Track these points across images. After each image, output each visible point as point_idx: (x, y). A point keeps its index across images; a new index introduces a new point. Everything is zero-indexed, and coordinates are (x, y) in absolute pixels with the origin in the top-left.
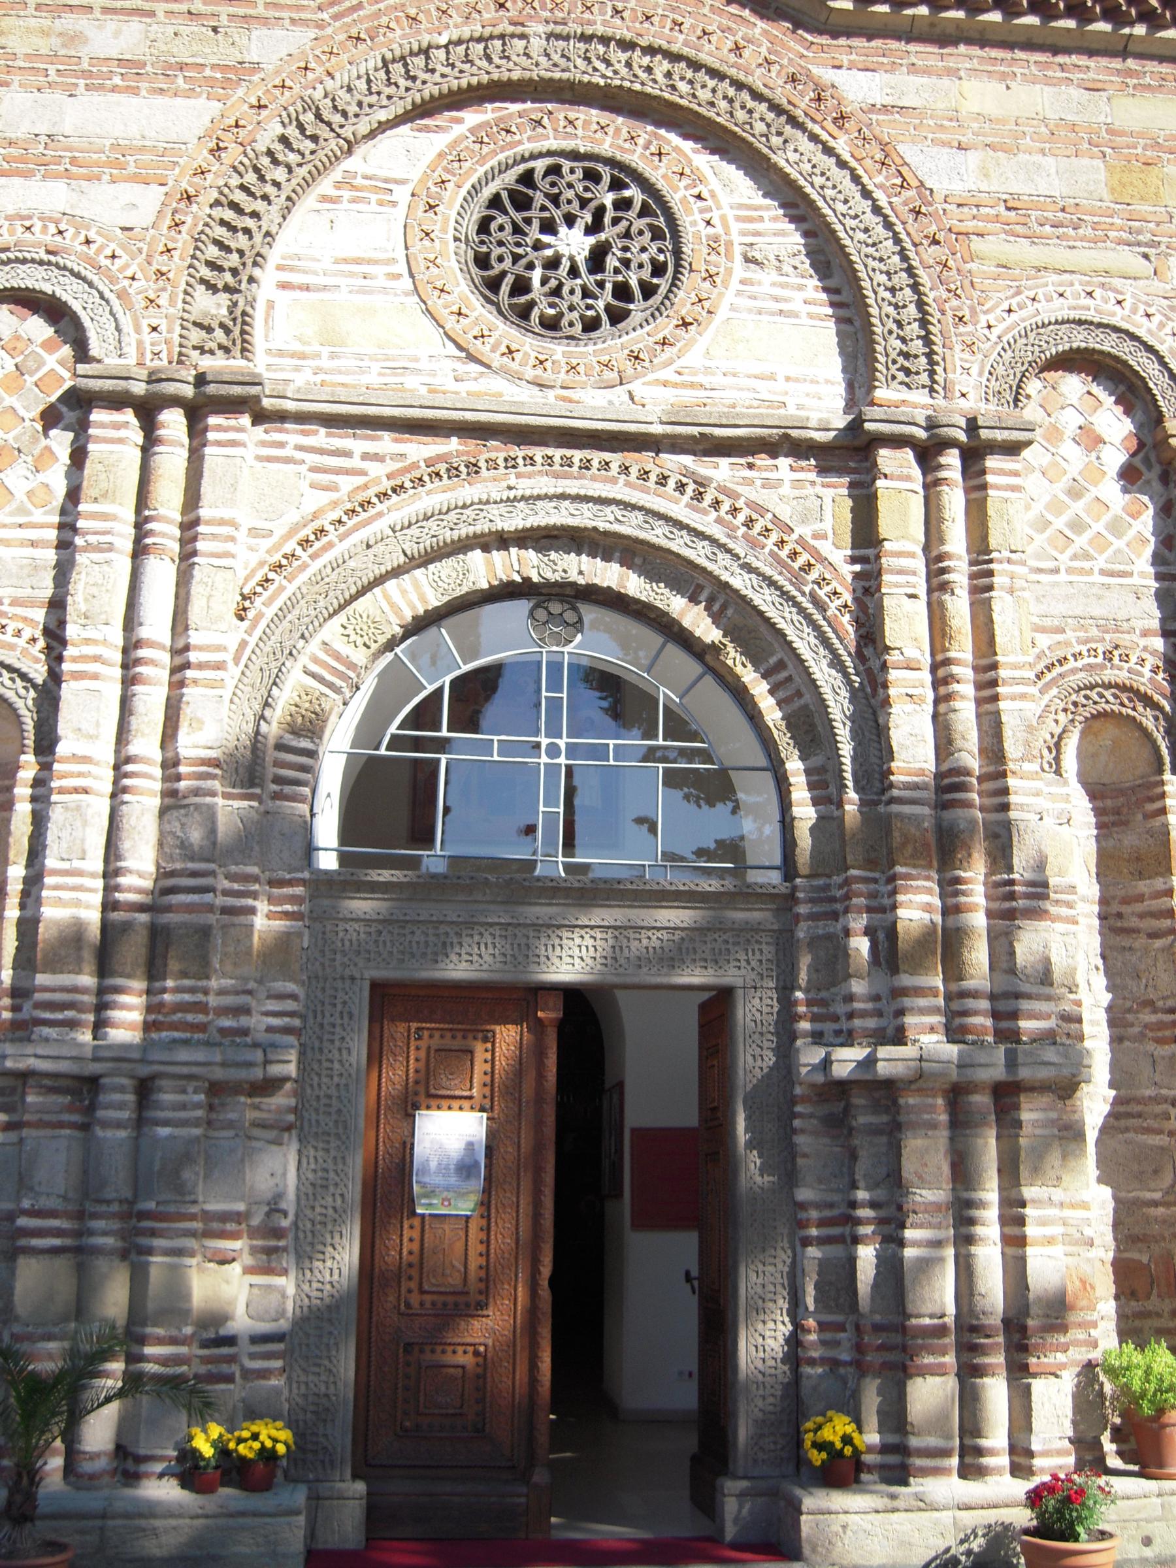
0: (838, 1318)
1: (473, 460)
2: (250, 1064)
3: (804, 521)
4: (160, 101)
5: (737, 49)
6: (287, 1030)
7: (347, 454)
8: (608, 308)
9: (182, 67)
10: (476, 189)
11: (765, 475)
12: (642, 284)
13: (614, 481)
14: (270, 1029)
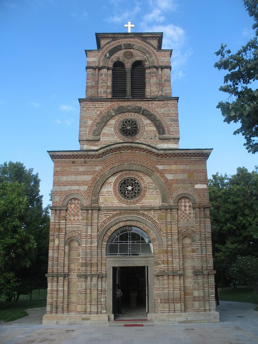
3: (154, 218)
4: (87, 176)
7: (108, 213)
8: (134, 195)
9: (89, 172)
10: (120, 183)
12: (137, 192)
13: (135, 215)
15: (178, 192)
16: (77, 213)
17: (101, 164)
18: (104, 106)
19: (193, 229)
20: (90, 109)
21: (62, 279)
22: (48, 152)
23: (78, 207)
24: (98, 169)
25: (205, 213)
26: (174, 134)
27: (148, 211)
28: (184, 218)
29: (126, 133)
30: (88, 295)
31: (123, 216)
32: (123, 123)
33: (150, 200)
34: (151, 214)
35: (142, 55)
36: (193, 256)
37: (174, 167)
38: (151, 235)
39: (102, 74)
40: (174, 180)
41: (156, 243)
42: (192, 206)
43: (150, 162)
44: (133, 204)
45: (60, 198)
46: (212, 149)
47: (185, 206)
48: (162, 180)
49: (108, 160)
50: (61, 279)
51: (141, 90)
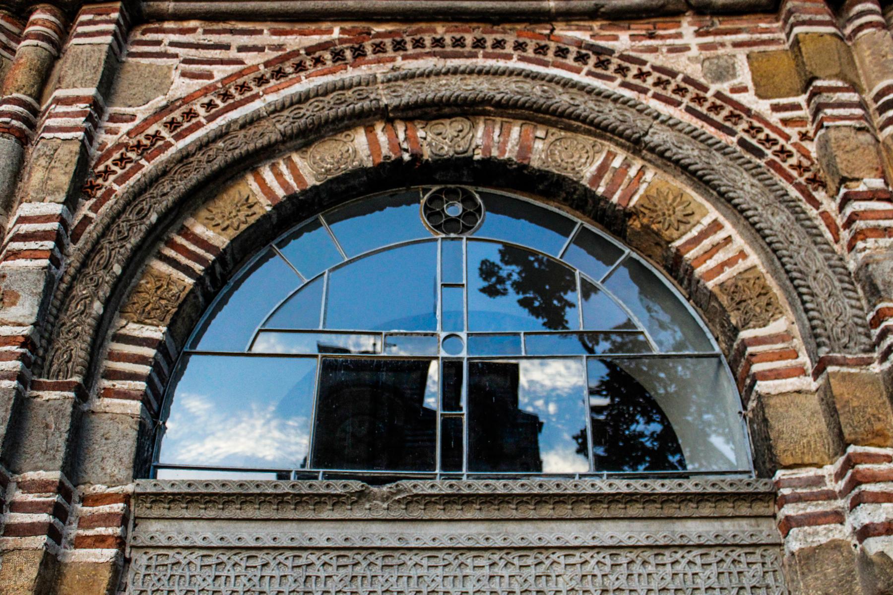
1: (356, 46)
3: (719, 77)
11: (669, 41)
13: (508, 57)
27: (640, 28)
31: (380, 71)
38: (707, 243)
41: (778, 326)
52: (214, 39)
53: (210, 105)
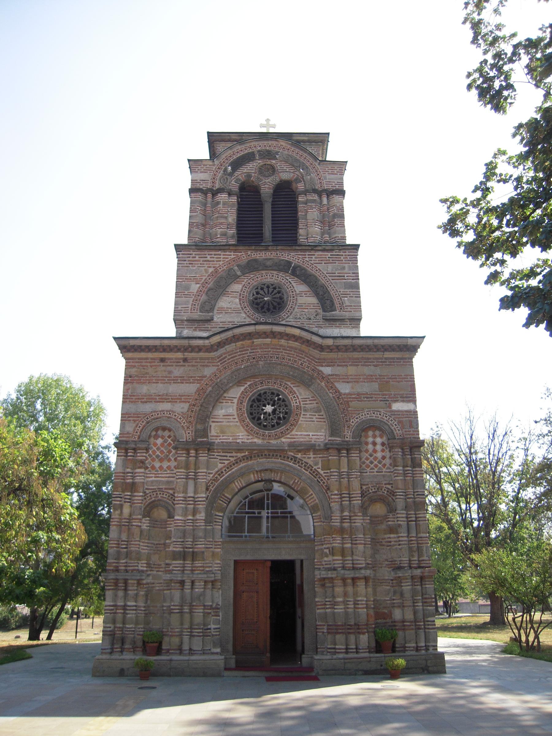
0: (324, 623)
2: (212, 577)
3: (315, 465)
4: (187, 384)
5: (302, 364)
6: (218, 570)
7: (227, 456)
8: (276, 422)
10: (250, 398)
14: (215, 570)
15: (360, 417)
16: (168, 456)
17: (214, 363)
18: (222, 259)
19: (389, 487)
20: (195, 264)
21: (134, 584)
22: (115, 339)
23: (170, 444)
24: (208, 371)
25: (413, 456)
26: (352, 310)
28: (372, 466)
29: (262, 308)
30: (187, 616)
31: (255, 462)
32: (257, 290)
33: (307, 432)
34: (309, 458)
35: (292, 171)
36: (389, 540)
37: (352, 370)
38: (310, 498)
39: (218, 203)
40: (351, 395)
41: (319, 514)
42: (388, 444)
43: (307, 360)
44: (275, 439)
45: (134, 425)
46: (424, 337)
47: (374, 444)
48: (331, 395)
49: (229, 355)
50: (132, 583)
51: (290, 232)
52: (224, 454)
53: (225, 470)
